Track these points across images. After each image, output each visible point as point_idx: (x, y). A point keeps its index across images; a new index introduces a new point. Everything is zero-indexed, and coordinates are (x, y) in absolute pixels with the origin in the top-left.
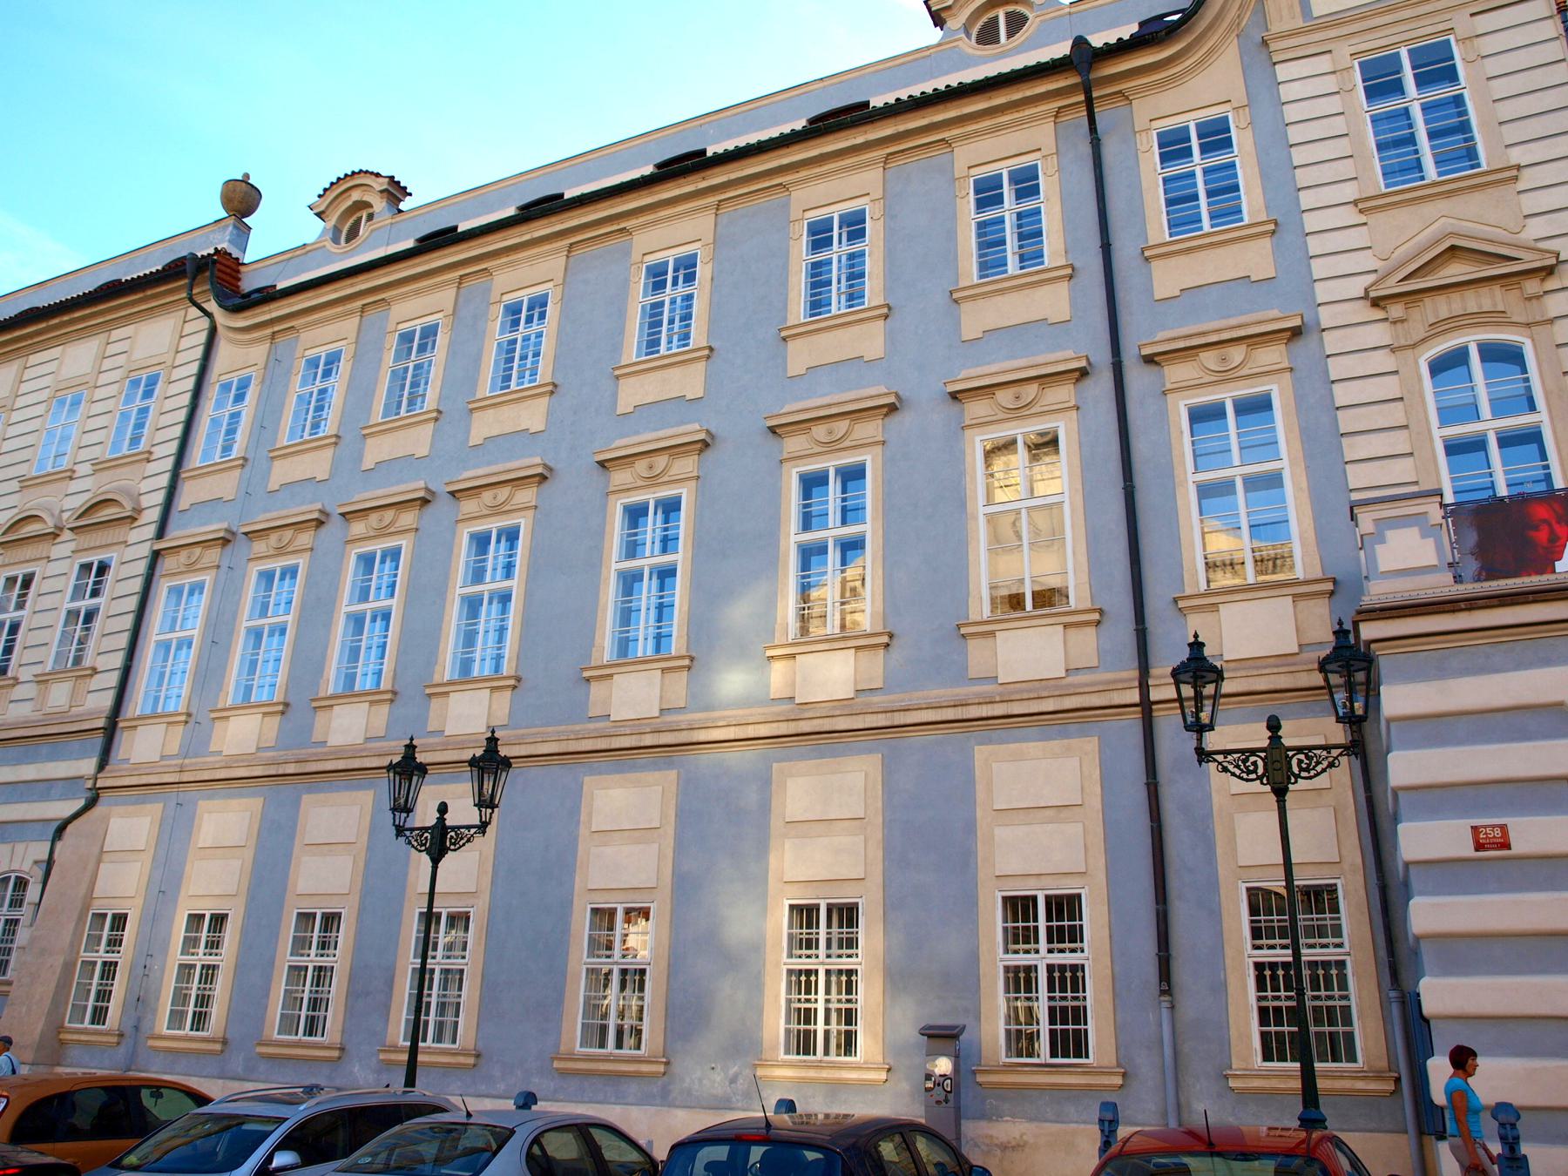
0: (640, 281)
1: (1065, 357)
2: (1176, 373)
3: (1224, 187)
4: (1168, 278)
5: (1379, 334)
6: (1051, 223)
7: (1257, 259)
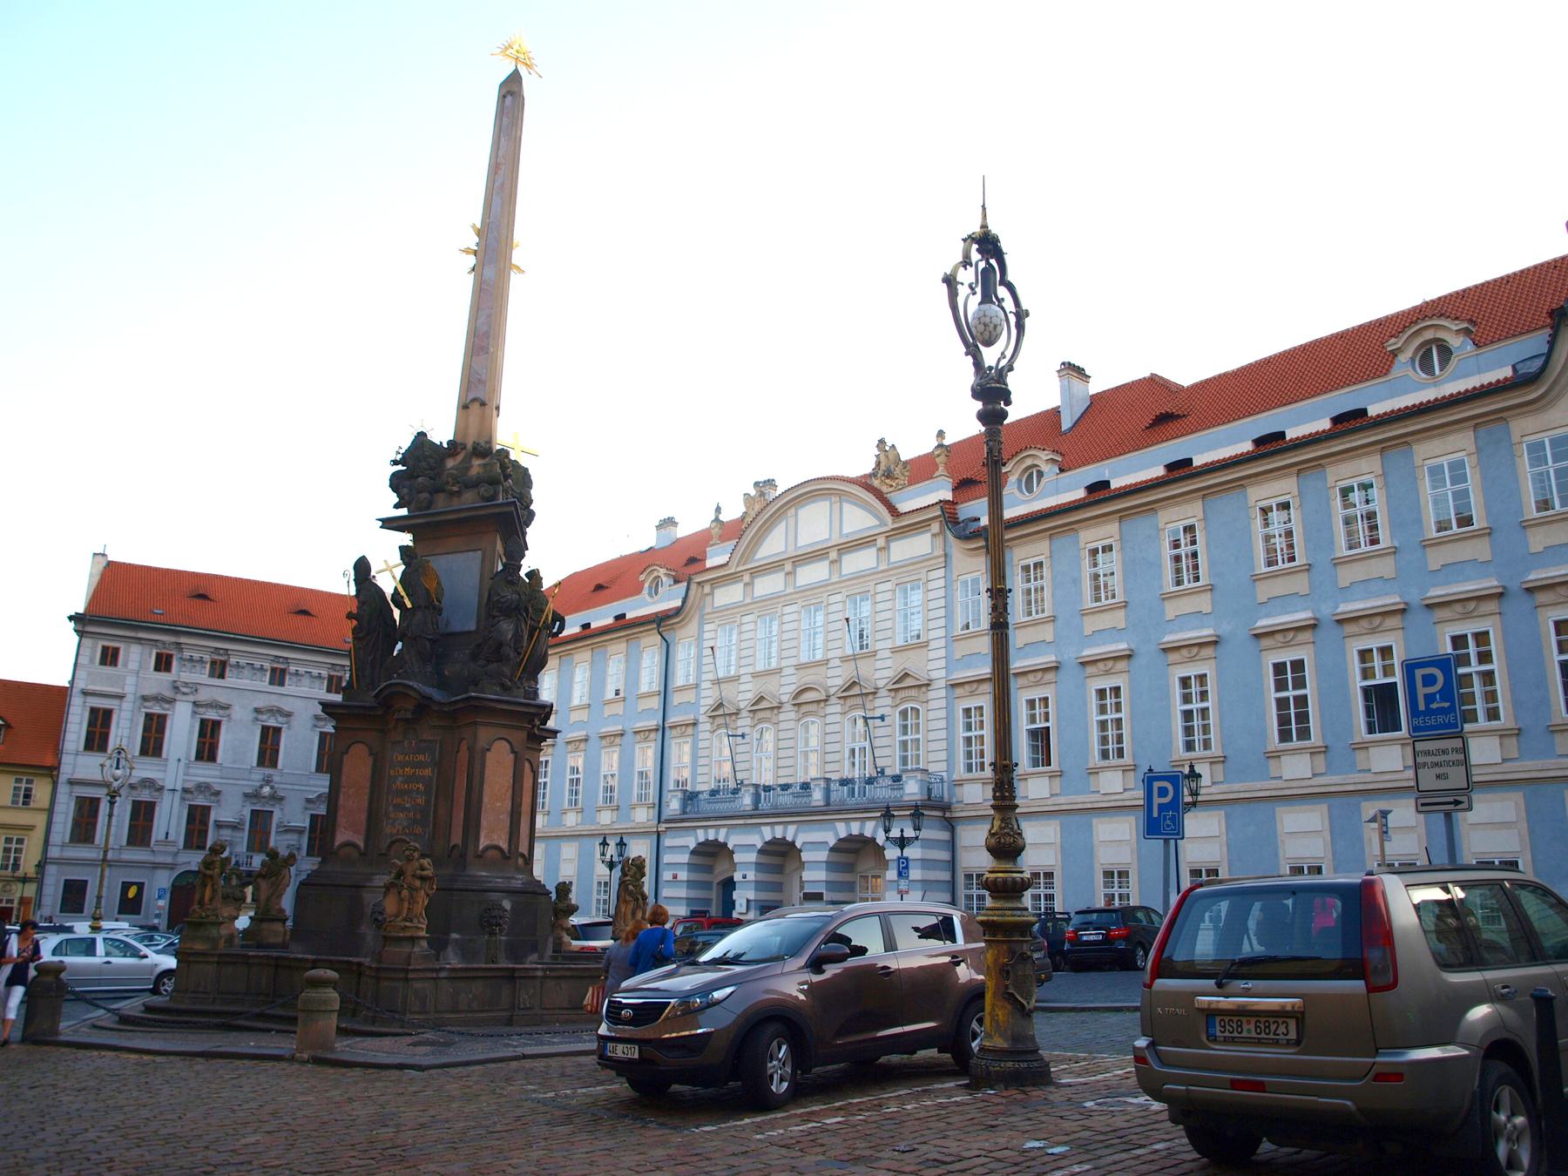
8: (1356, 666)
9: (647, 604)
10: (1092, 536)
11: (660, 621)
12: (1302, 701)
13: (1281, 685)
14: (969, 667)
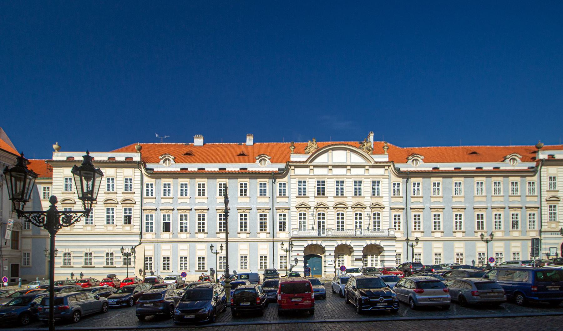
0: (218, 186)
1: (268, 207)
2: (278, 211)
3: (284, 192)
4: (278, 200)
5: (296, 210)
6: (267, 191)
7: (286, 200)
8: (494, 217)
9: (259, 167)
10: (434, 180)
11: (273, 176)
12: (482, 222)
13: (478, 219)
14: (396, 205)
